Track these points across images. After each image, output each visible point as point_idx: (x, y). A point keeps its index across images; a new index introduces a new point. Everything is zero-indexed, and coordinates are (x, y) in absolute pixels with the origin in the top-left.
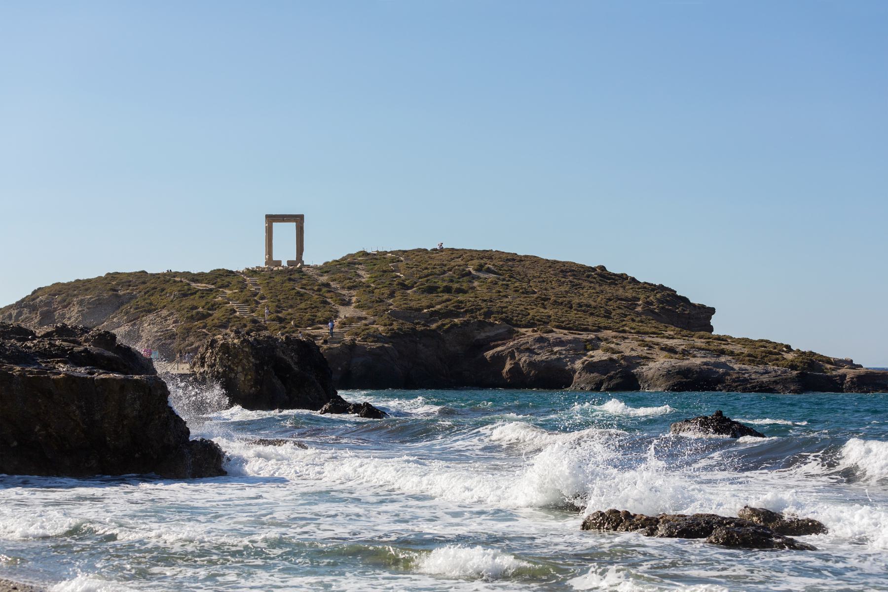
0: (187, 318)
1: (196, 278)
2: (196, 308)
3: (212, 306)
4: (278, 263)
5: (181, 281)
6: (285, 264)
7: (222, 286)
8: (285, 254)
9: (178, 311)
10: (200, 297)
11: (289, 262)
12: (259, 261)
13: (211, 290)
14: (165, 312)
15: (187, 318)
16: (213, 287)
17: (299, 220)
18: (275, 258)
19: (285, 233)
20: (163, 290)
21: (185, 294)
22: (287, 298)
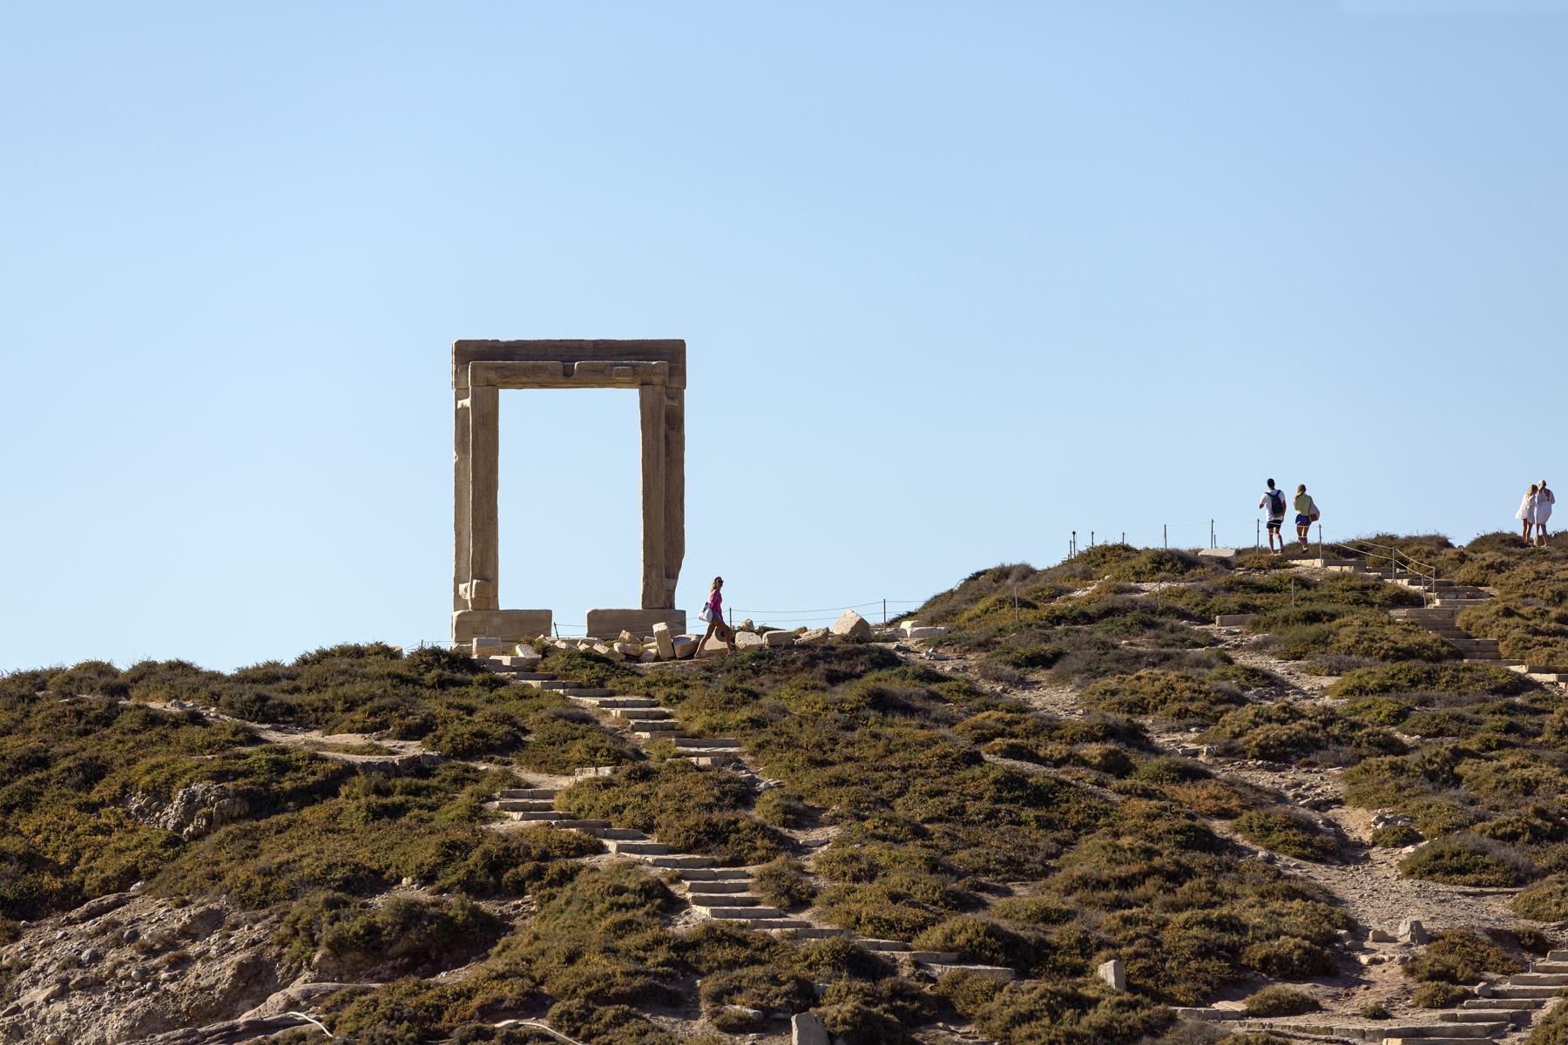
0: (339, 946)
1: (276, 694)
2: (379, 881)
3: (496, 865)
5: (195, 719)
6: (570, 627)
7: (481, 747)
9: (255, 900)
10: (376, 814)
12: (417, 614)
13: (417, 767)
14: (152, 913)
15: (339, 946)
16: (413, 749)
17: (654, 370)
18: (510, 598)
19: (572, 449)
20: (94, 772)
21: (266, 798)
22: (958, 812)
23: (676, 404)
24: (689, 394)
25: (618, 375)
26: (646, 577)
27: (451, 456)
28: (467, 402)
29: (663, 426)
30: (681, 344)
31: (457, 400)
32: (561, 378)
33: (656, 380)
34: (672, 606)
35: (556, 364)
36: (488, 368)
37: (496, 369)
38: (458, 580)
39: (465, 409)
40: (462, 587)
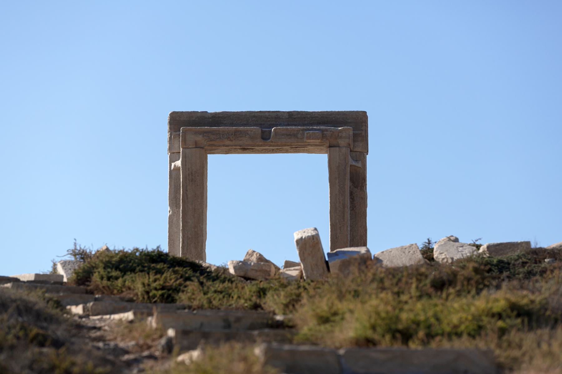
23: (359, 165)
24: (370, 159)
25: (309, 138)
27: (166, 211)
28: (179, 163)
29: (348, 183)
31: (171, 161)
32: (259, 141)
33: (342, 142)
35: (257, 130)
36: (196, 133)
37: (204, 133)
39: (177, 169)
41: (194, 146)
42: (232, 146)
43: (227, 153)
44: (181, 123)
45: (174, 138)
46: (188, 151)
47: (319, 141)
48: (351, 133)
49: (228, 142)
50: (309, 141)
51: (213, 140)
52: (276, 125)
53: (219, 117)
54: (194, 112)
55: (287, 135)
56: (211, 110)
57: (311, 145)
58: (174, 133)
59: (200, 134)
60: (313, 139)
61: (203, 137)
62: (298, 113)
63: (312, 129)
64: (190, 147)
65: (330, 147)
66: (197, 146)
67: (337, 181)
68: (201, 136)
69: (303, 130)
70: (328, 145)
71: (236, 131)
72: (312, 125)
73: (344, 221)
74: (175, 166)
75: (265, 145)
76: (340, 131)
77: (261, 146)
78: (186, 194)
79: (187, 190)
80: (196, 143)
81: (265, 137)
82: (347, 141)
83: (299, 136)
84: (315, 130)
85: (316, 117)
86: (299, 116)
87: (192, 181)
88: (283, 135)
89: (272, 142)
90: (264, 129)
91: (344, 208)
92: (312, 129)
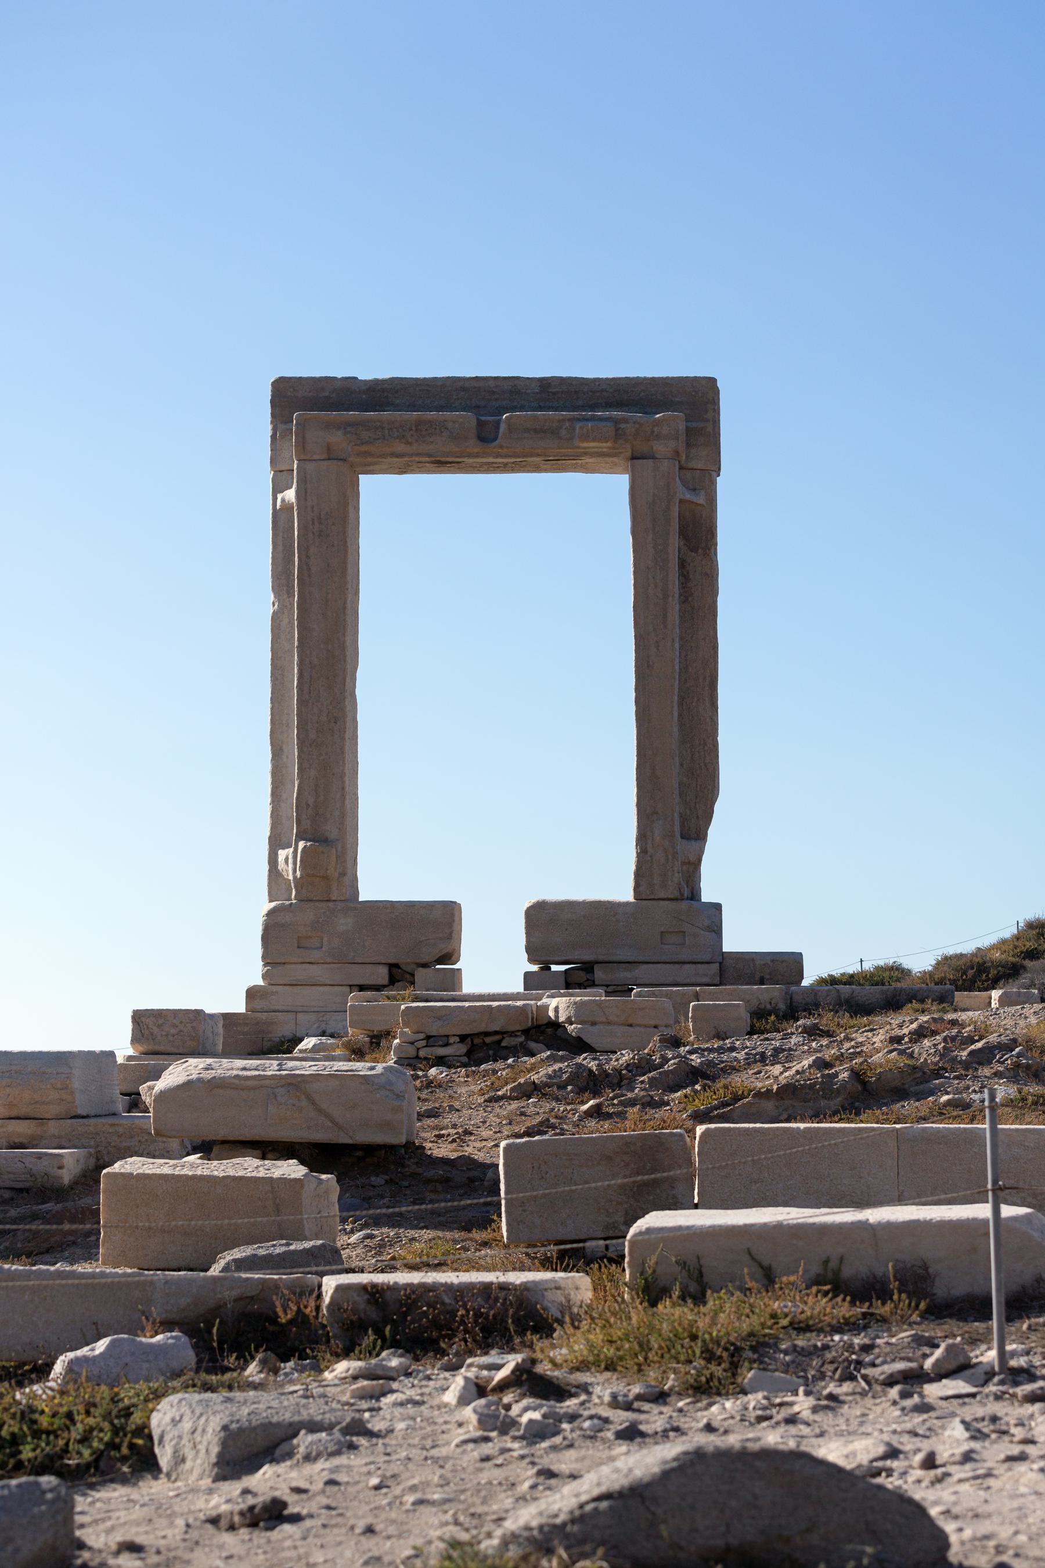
4: (426, 935)
8: (499, 818)
11: (552, 929)
23: (701, 500)
24: (725, 486)
25: (586, 438)
26: (642, 838)
28: (290, 495)
29: (675, 542)
30: (713, 381)
31: (277, 489)
33: (660, 448)
34: (694, 894)
35: (466, 419)
36: (329, 426)
37: (346, 426)
38: (276, 842)
39: (287, 507)
40: (282, 854)
41: (325, 456)
42: (412, 455)
43: (402, 471)
44: (300, 403)
45: (282, 437)
46: (310, 467)
47: (609, 444)
48: (682, 426)
49: (401, 448)
50: (585, 445)
51: (367, 443)
52: (513, 409)
53: (383, 391)
54: (327, 378)
55: (536, 431)
56: (366, 374)
57: (592, 455)
58: (281, 427)
59: (339, 428)
60: (594, 440)
61: (345, 434)
62: (562, 380)
63: (593, 419)
64: (316, 457)
65: (633, 458)
66: (331, 455)
67: (651, 536)
68: (339, 433)
69: (572, 420)
70: (629, 454)
71: (420, 422)
72: (593, 407)
73: (665, 627)
74: (283, 500)
75: (485, 455)
76: (658, 422)
77: (477, 456)
78: (307, 564)
79: (308, 557)
80: (329, 448)
81: (486, 435)
82: (672, 444)
83: (563, 432)
84: (601, 419)
85: (603, 390)
86: (564, 388)
87: (320, 536)
88: (527, 430)
89: (501, 447)
90: (483, 418)
91: (666, 596)
92: (593, 419)
